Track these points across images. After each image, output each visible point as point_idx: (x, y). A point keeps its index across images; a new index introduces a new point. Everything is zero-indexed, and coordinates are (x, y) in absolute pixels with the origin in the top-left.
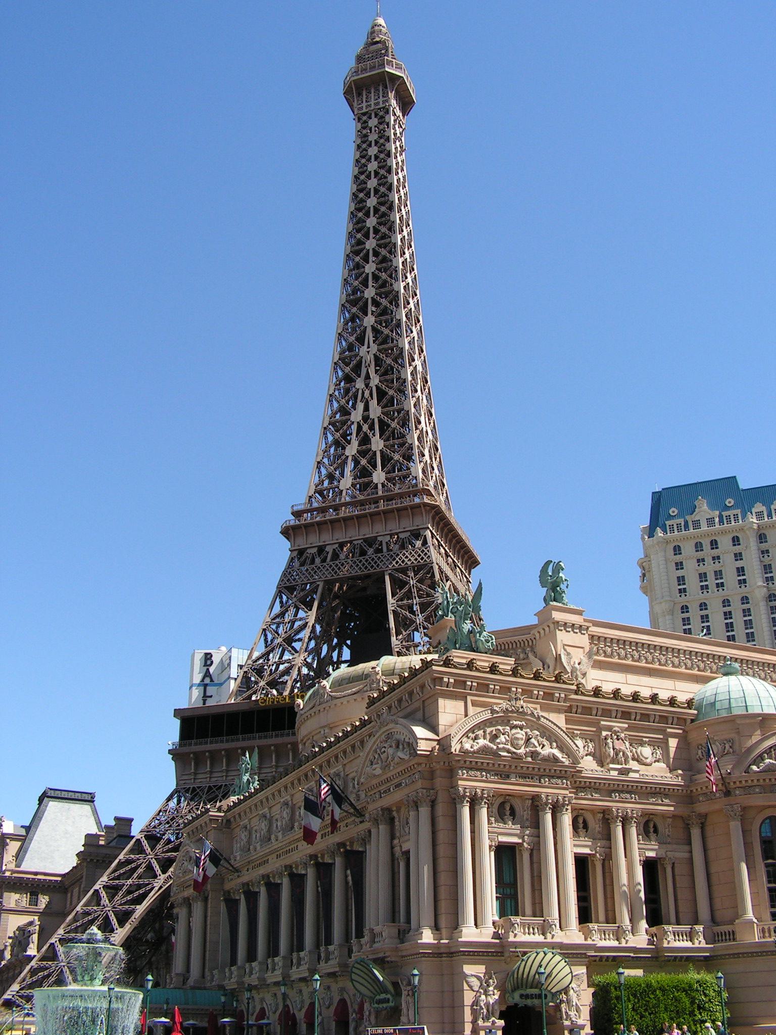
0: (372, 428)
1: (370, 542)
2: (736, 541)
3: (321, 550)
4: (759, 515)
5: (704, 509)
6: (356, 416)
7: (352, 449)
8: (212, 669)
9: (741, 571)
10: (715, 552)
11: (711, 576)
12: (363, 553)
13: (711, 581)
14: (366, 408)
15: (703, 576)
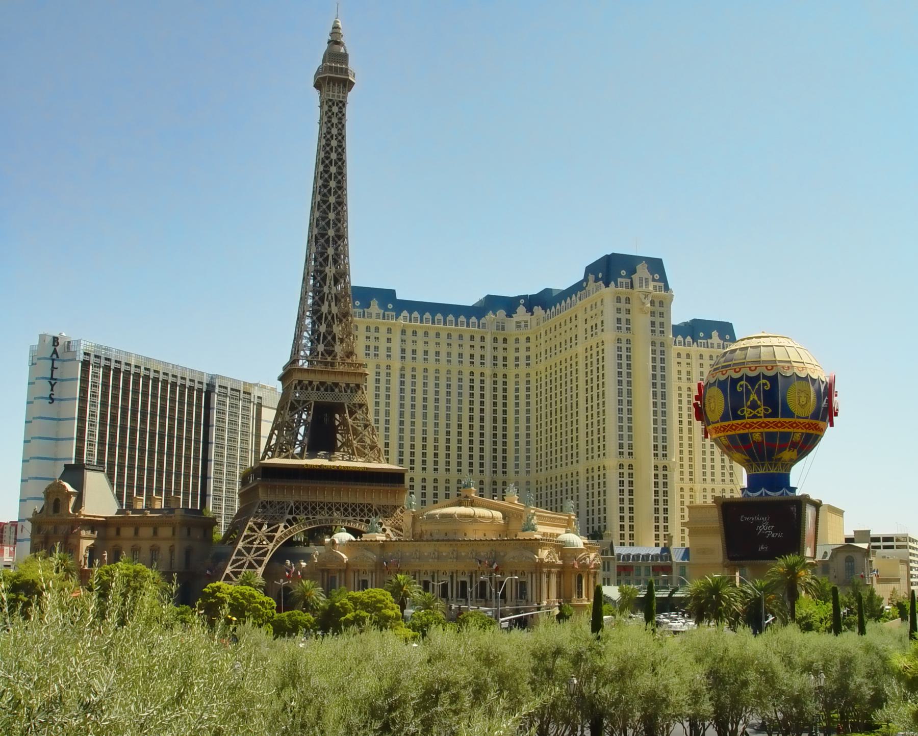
0: (333, 318)
1: (336, 385)
2: (389, 330)
3: (311, 383)
4: (405, 318)
5: (375, 307)
6: (324, 309)
7: (323, 328)
8: (58, 348)
9: (389, 349)
10: (377, 335)
11: (372, 348)
12: (333, 390)
13: (372, 352)
14: (330, 306)
15: (368, 347)
